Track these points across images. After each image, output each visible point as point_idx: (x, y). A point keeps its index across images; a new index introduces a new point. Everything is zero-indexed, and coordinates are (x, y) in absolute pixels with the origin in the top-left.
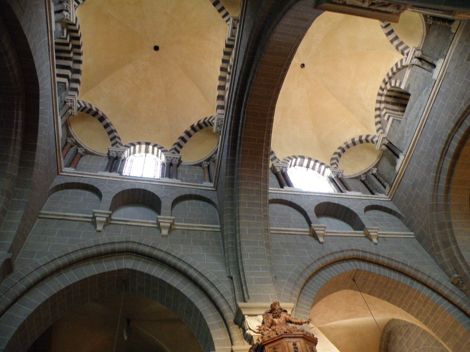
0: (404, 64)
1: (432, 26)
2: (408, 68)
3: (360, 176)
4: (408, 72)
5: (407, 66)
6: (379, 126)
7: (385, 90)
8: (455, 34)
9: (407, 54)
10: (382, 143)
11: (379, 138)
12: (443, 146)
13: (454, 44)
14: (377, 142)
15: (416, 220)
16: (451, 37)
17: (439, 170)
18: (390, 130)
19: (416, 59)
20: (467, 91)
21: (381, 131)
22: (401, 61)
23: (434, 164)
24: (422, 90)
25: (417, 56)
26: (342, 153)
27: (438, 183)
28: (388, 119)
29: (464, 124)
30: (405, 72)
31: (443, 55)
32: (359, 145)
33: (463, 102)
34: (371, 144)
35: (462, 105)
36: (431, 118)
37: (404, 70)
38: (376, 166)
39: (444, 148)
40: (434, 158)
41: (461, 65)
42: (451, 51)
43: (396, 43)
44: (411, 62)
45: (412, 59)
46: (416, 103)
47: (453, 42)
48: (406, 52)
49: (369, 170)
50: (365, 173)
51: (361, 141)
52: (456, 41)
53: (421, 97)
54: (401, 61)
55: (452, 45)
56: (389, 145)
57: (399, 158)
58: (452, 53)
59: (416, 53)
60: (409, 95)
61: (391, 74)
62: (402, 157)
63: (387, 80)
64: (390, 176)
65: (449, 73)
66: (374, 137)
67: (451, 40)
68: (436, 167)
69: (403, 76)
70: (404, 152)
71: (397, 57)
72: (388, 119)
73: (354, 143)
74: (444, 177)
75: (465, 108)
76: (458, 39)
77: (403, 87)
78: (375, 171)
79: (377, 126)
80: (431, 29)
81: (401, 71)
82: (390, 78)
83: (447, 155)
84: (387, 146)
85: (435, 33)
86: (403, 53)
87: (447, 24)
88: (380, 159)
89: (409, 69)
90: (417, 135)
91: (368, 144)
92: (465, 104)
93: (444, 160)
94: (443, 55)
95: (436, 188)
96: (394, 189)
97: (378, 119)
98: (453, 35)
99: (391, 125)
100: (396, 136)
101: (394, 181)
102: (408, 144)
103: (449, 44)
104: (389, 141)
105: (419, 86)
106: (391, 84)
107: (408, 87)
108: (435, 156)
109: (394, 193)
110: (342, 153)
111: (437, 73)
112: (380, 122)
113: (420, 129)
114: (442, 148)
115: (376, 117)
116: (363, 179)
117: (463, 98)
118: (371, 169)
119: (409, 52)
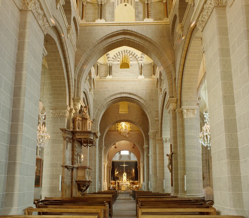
0: (138, 59)
2: (137, 62)
4: (136, 62)
6: (114, 58)
9: (141, 60)
14: (109, 60)
18: (115, 64)
21: (113, 60)
22: (139, 58)
28: (119, 61)
30: (135, 61)
37: (136, 60)
42: (147, 79)
52: (150, 79)
54: (139, 58)
56: (111, 67)
57: (110, 75)
60: (129, 68)
61: (133, 54)
63: (131, 53)
69: (134, 61)
70: (113, 78)
72: (119, 61)
77: (131, 62)
78: (99, 65)
84: (110, 66)
86: (141, 57)
91: (107, 58)
97: (116, 56)
99: (117, 64)
100: (115, 69)
102: (116, 78)
106: (130, 55)
107: (131, 66)
115: (117, 54)
119: (143, 60)
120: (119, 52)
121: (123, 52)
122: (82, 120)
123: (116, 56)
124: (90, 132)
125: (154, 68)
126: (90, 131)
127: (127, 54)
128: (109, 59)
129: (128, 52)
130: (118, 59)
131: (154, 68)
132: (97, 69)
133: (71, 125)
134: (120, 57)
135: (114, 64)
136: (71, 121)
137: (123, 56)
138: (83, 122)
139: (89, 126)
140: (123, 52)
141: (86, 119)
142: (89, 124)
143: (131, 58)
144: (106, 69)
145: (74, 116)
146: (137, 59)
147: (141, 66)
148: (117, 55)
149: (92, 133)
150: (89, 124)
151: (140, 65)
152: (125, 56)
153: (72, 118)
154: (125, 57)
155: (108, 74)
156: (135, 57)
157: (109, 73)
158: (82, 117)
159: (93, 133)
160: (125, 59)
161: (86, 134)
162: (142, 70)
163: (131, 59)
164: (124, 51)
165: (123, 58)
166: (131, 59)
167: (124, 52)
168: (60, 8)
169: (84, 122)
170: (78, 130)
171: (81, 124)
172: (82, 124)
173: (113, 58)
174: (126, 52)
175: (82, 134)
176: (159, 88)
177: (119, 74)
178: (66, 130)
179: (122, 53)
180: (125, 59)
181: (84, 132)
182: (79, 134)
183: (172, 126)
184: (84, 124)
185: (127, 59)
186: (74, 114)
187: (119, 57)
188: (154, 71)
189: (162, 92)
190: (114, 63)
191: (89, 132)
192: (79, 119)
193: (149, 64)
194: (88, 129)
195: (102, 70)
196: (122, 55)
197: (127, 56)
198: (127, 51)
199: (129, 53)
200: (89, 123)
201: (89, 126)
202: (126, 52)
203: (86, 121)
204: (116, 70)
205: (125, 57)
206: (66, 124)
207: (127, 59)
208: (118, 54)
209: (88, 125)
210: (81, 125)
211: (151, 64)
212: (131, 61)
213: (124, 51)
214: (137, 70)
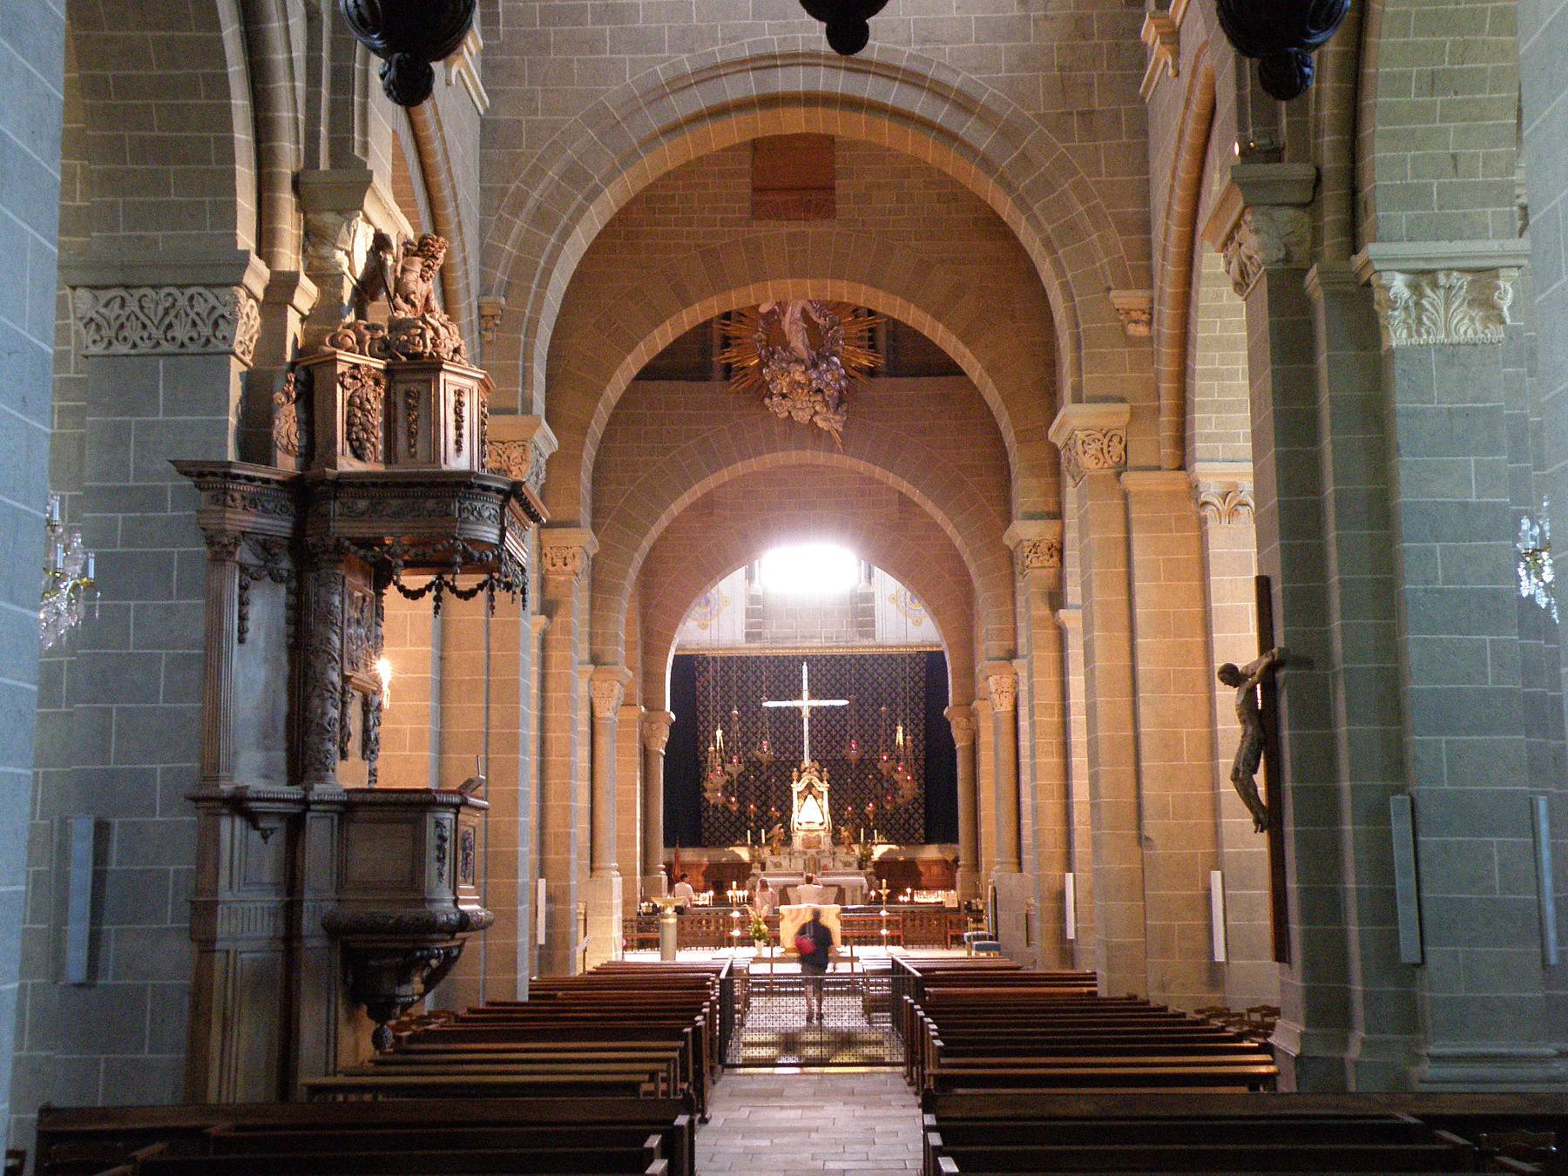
12: (777, 50)
15: (526, 87)
17: (709, 74)
20: (945, 43)
23: (716, 48)
27: (673, 92)
29: (861, 77)
33: (913, 48)
35: (908, 50)
39: (774, 57)
40: (731, 40)
68: (711, 62)
74: (700, 99)
75: (904, 64)
83: (757, 73)
92: (912, 57)
93: (741, 71)
95: (658, 94)
108: (735, 39)
114: (770, 50)
117: (925, 41)
122: (388, 371)
124: (463, 484)
126: (470, 473)
133: (286, 424)
136: (279, 382)
138: (401, 388)
139: (459, 427)
141: (432, 367)
142: (459, 404)
145: (306, 333)
149: (487, 489)
150: (459, 404)
153: (289, 358)
158: (385, 349)
159: (499, 491)
161: (430, 504)
169: (408, 394)
170: (347, 464)
171: (377, 405)
172: (389, 404)
175: (394, 502)
178: (238, 476)
181: (410, 485)
182: (362, 504)
183: (1268, 411)
184: (409, 408)
186: (304, 319)
191: (458, 484)
192: (356, 366)
194: (452, 446)
200: (459, 393)
201: (459, 427)
203: (428, 381)
206: (233, 420)
209: (451, 418)
210: (378, 420)
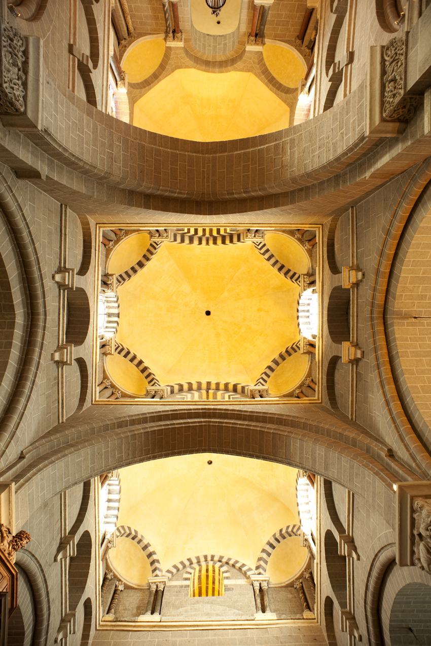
0: (249, 573)
1: (293, 589)
2: (246, 580)
3: (111, 571)
4: (242, 581)
5: (248, 578)
6: (174, 571)
7: (212, 562)
8: (304, 619)
9: (260, 574)
10: (158, 583)
11: (162, 577)
13: (294, 623)
14: (156, 576)
16: (298, 616)
18: (176, 586)
19: (259, 585)
21: (170, 575)
22: (250, 569)
24: (234, 608)
25: (262, 585)
26: (131, 536)
30: (241, 579)
31: (280, 616)
32: (145, 554)
34: (151, 569)
36: (215, 635)
37: (242, 576)
38: (127, 587)
41: (281, 643)
43: (265, 556)
44: (255, 581)
45: (258, 581)
46: (220, 607)
47: (295, 621)
48: (261, 570)
49: (120, 580)
50: (115, 576)
51: (150, 555)
52: (299, 623)
53: (229, 610)
54: (250, 569)
55: (293, 620)
56: (160, 593)
57: (152, 613)
58: (287, 625)
59: (264, 582)
61: (231, 562)
62: (156, 617)
63: (224, 560)
64: (123, 611)
65: (268, 632)
66: (160, 570)
67: (297, 617)
69: (236, 578)
71: (251, 563)
73: (145, 548)
76: (299, 625)
78: (121, 588)
79: (173, 568)
80: (290, 588)
81: (239, 574)
82: (227, 563)
84: (157, 591)
85: (290, 596)
86: (257, 568)
87: (305, 604)
88: (136, 589)
89: (246, 582)
90: (191, 626)
94: (280, 616)
96: (115, 626)
97: (180, 567)
98: (302, 618)
99: (182, 587)
100: (174, 598)
101: (125, 621)
102: (176, 619)
103: (292, 617)
104: (164, 590)
105: (237, 601)
106: (221, 566)
109: (109, 628)
110: (131, 536)
111: (260, 616)
112: (178, 570)
113: (198, 626)
115: (182, 563)
116: (109, 576)
118: (122, 582)
119: (262, 574)
120: (189, 560)
121: (202, 559)
123: (180, 567)
125: (304, 593)
127: (215, 563)
128: (157, 572)
129: (216, 559)
130: (188, 576)
131: (304, 593)
132: (113, 598)
134: (192, 571)
135: (170, 586)
137: (200, 571)
140: (202, 559)
143: (226, 572)
144: (142, 600)
146: (245, 574)
147: (261, 590)
148: (184, 566)
151: (257, 588)
152: (207, 571)
154: (207, 576)
155: (147, 611)
156: (240, 569)
157: (150, 607)
160: (207, 583)
162: (266, 598)
163: (226, 575)
164: (206, 557)
165: (200, 577)
166: (226, 575)
167: (206, 560)
168: (61, 559)
173: (168, 571)
174: (209, 558)
176: (343, 613)
177: (186, 611)
179: (199, 562)
180: (207, 583)
185: (214, 583)
187: (189, 570)
188: (306, 600)
189: (357, 628)
190: (171, 584)
193: (287, 586)
195: (130, 601)
196: (197, 568)
197: (214, 571)
198: (213, 557)
199: (220, 561)
202: (209, 558)
204: (177, 602)
205: (207, 576)
207: (214, 583)
208: (187, 563)
211: (291, 585)
212: (227, 578)
213: (206, 557)
214: (249, 598)
